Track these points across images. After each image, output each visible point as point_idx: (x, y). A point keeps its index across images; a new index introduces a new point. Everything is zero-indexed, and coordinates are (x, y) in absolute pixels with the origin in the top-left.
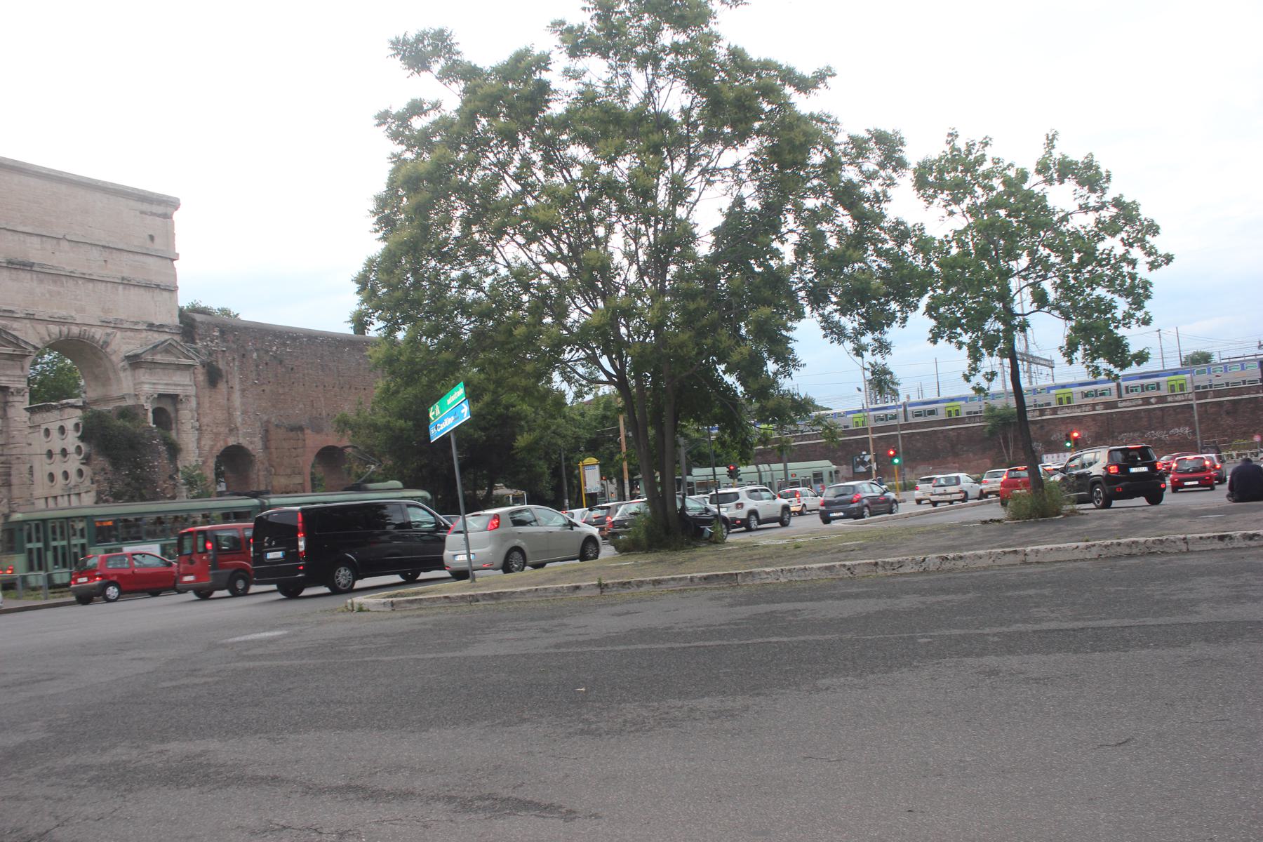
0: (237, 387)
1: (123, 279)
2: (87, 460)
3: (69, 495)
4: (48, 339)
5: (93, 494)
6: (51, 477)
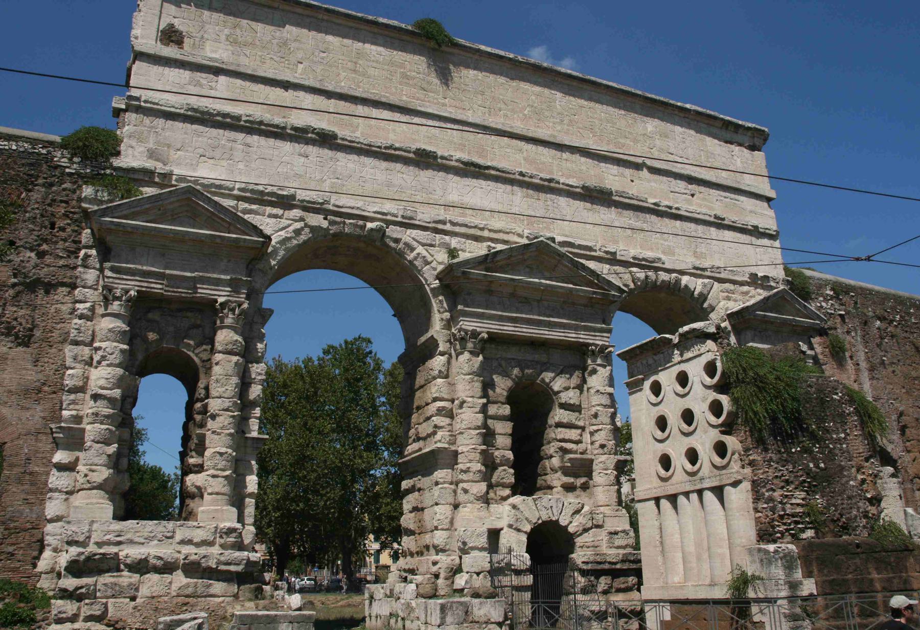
0: (863, 365)
1: (716, 217)
2: (728, 428)
3: (700, 492)
4: (632, 286)
5: (746, 486)
6: (666, 462)
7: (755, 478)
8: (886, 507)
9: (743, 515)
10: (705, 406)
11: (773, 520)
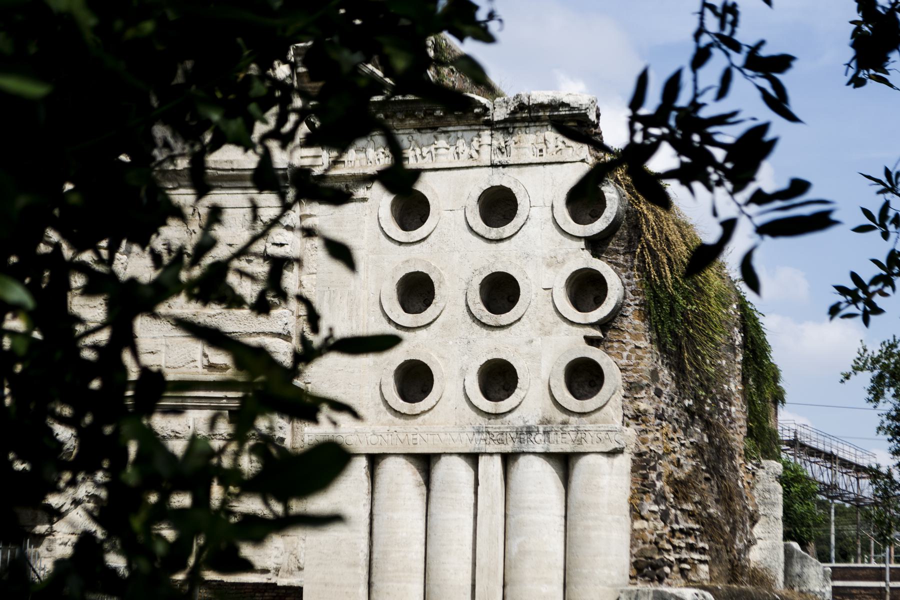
3: (508, 459)
5: (624, 462)
7: (643, 448)
8: (762, 536)
9: (618, 521)
10: (559, 281)
11: (661, 536)
